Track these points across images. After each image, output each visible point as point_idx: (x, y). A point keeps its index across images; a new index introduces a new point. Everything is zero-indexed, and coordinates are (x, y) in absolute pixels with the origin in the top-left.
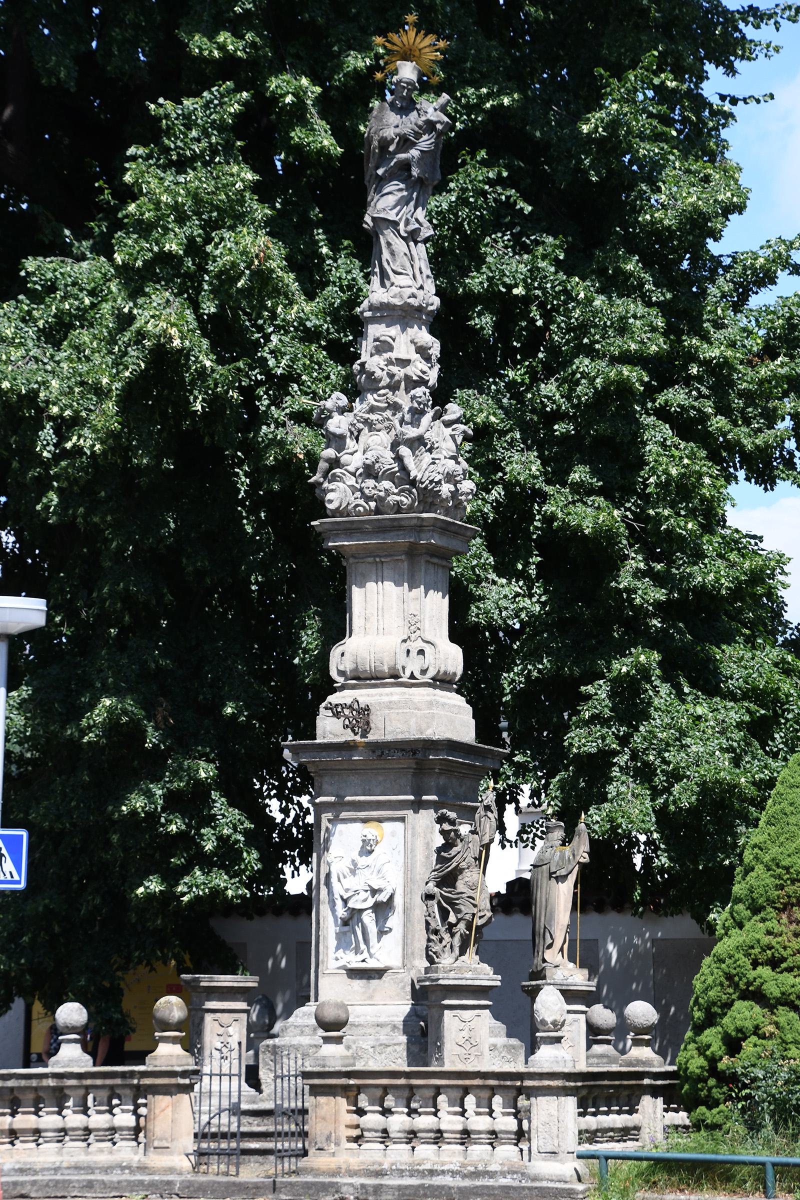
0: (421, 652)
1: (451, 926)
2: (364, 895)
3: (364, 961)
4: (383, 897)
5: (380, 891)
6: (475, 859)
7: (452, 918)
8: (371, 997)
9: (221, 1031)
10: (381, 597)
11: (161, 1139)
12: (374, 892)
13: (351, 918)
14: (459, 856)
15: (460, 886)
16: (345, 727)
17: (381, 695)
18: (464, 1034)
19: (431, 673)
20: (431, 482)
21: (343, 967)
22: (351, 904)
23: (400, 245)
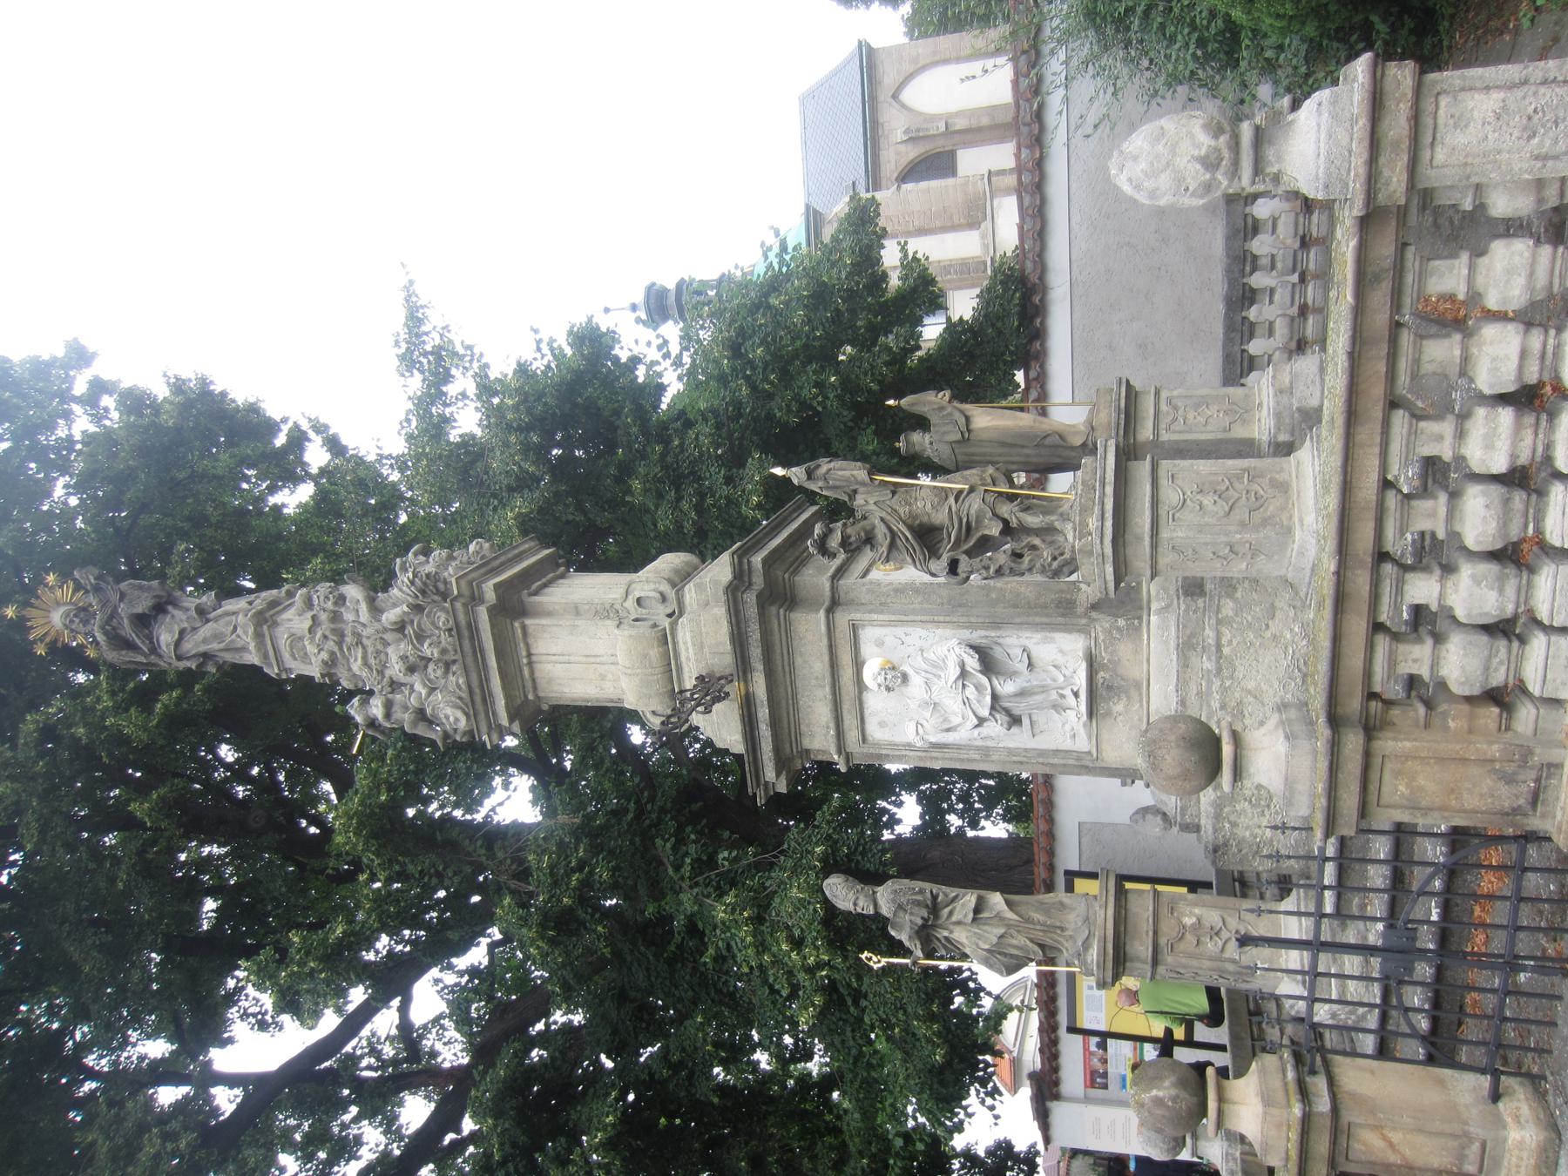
0: (639, 601)
1: (1007, 530)
2: (971, 692)
3: (1076, 695)
4: (972, 663)
5: (962, 665)
6: (894, 493)
7: (994, 530)
8: (1138, 685)
9: (1190, 938)
10: (572, 659)
11: (1461, 1157)
12: (964, 674)
13: (1008, 712)
14: (888, 518)
15: (940, 517)
16: (708, 711)
17: (688, 659)
18: (1207, 501)
19: (665, 588)
20: (412, 583)
21: (1088, 726)
22: (985, 713)
23: (206, 630)
